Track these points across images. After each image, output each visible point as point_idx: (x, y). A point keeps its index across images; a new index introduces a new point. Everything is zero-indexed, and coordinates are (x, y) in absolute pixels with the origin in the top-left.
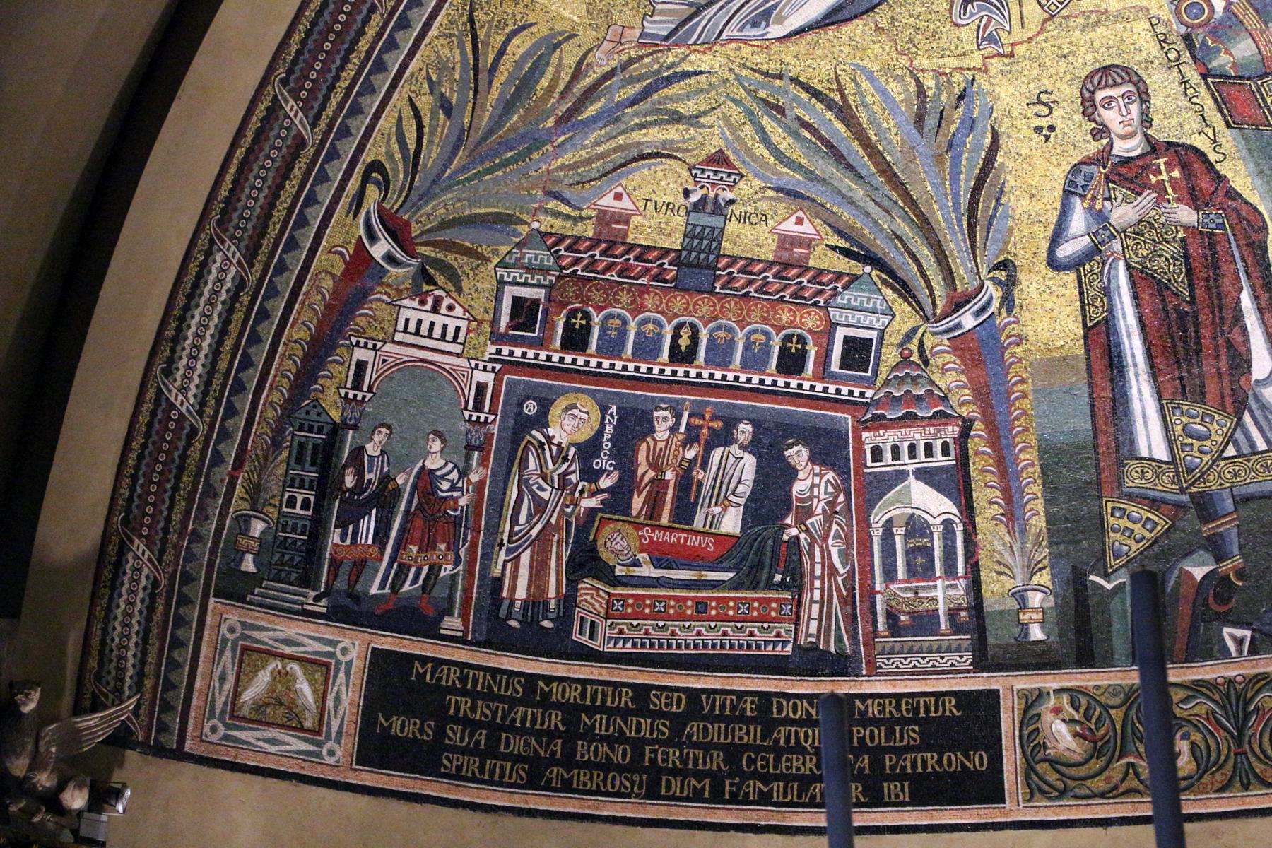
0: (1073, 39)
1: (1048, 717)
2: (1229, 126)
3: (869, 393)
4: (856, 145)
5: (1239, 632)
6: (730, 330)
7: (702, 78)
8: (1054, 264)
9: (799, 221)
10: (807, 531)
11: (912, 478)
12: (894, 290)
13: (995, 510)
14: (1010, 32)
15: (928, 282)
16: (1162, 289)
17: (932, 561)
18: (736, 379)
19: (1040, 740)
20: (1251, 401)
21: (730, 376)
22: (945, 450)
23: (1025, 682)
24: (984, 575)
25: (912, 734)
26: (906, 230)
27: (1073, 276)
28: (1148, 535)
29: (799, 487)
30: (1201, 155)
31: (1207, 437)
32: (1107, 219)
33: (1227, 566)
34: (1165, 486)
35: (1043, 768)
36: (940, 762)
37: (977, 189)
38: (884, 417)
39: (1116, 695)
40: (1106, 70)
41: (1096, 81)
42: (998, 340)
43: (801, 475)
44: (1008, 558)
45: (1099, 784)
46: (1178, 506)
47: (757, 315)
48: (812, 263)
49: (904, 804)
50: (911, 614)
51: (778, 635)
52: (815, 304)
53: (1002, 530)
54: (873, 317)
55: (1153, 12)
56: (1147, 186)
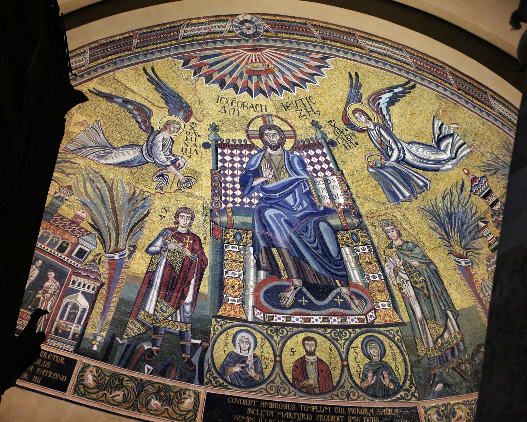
1: (88, 372)
2: (211, 236)
3: (79, 265)
4: (109, 199)
5: (150, 367)
6: (49, 234)
7: (76, 165)
8: (147, 251)
9: (83, 212)
10: (44, 297)
11: (80, 293)
12: (100, 240)
13: (100, 310)
15: (111, 242)
16: (173, 269)
17: (75, 318)
18: (44, 248)
19: (83, 378)
20: (181, 307)
21: (43, 246)
22: (93, 290)
23: (86, 360)
24: (88, 327)
25: (49, 364)
26: (111, 226)
27: (151, 256)
28: (138, 332)
29: (47, 284)
30: (200, 240)
31: (166, 312)
32: (167, 245)
33: (155, 348)
34: (148, 321)
35: (81, 386)
36: (52, 375)
37: (136, 224)
38: (80, 273)
39: (109, 373)
42: (122, 265)
43: (49, 281)
44: (97, 325)
45: (94, 396)
46: (149, 327)
47: (59, 232)
48: (81, 225)
49: (37, 384)
50: (63, 331)
51: (23, 323)
52: (76, 236)
53: (99, 317)
54: (90, 245)
56: (182, 241)
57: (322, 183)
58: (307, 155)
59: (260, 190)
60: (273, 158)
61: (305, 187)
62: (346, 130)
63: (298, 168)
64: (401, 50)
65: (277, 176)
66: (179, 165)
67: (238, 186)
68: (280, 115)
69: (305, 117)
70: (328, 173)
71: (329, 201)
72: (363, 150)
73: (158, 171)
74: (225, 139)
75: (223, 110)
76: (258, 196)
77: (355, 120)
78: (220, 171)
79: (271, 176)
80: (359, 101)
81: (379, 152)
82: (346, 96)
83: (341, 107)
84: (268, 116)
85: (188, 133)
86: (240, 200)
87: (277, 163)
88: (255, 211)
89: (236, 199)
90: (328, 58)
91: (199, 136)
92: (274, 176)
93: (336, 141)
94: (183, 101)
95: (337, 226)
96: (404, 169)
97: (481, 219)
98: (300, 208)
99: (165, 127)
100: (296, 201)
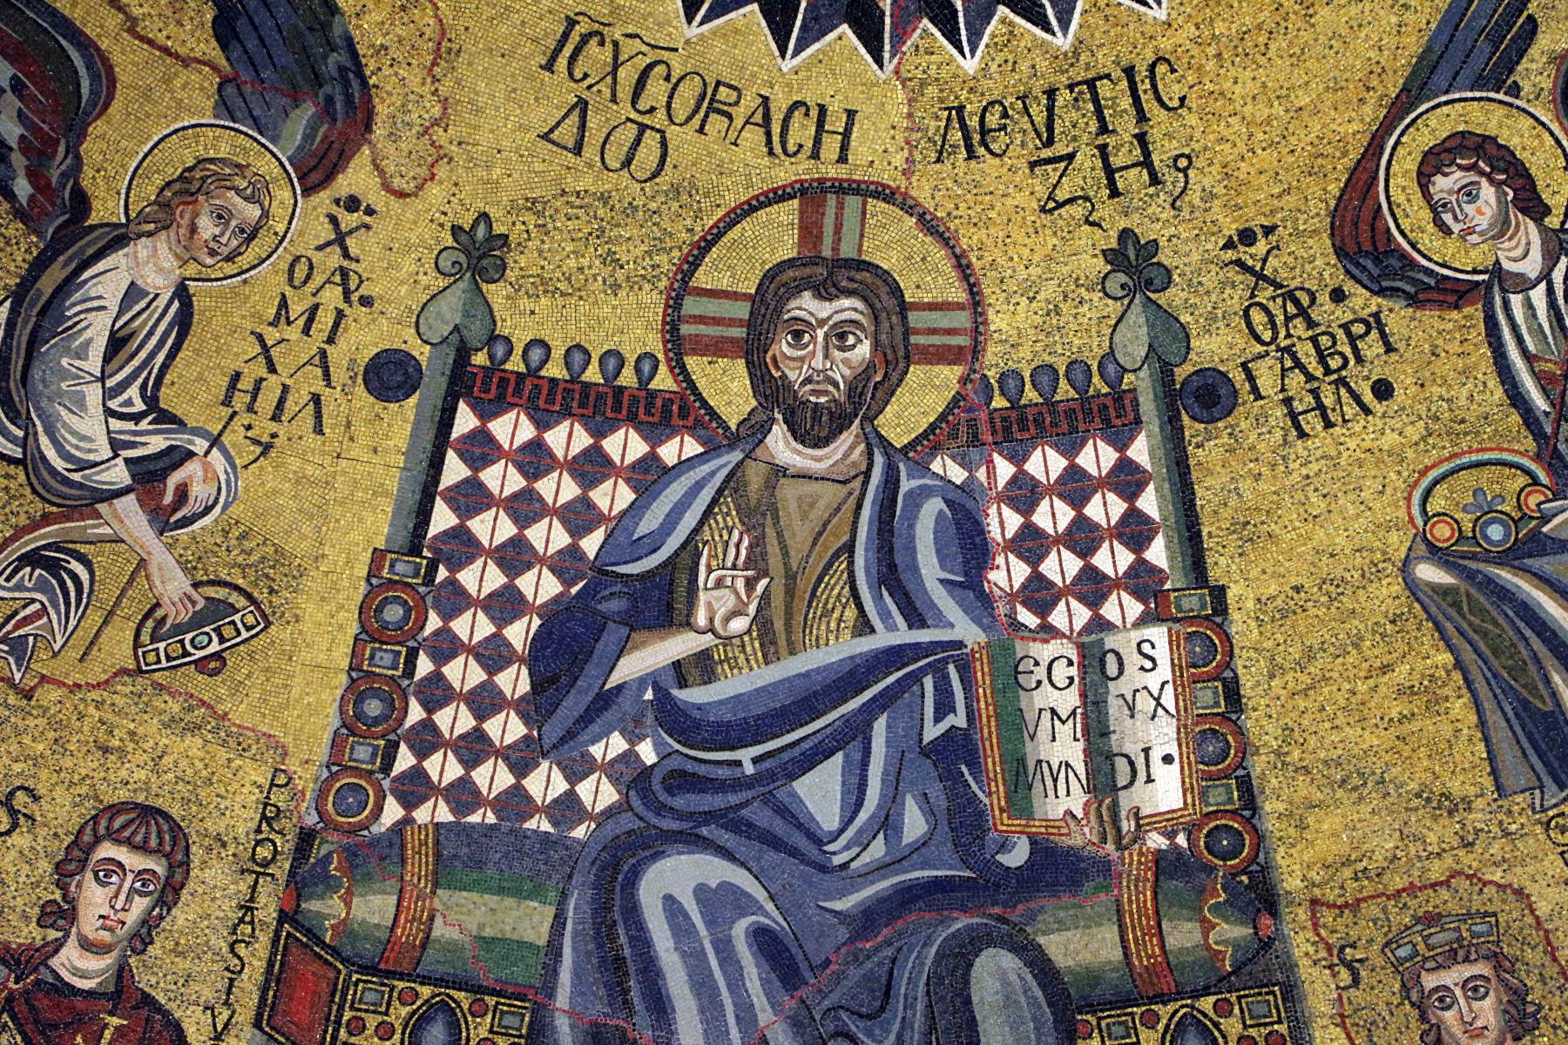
0: (141, 731)
2: (257, 1024)
14: (55, 655)
40: (148, 813)
41: (117, 824)
55: (292, 765)
57: (1061, 672)
58: (1013, 481)
59: (650, 719)
60: (789, 492)
61: (944, 707)
62: (1338, 296)
63: (930, 569)
65: (779, 625)
66: (182, 494)
67: (515, 681)
68: (922, 192)
69: (1078, 210)
70: (1122, 608)
71: (1076, 801)
72: (1414, 433)
73: (34, 526)
74: (520, 340)
75: (567, 133)
76: (629, 757)
77: (1426, 214)
78: (432, 567)
79: (739, 625)
81: (1530, 444)
82: (1414, 45)
83: (1354, 126)
84: (843, 188)
85: (300, 272)
86: (505, 779)
87: (799, 534)
88: (583, 864)
89: (481, 776)
91: (366, 301)
92: (762, 622)
93: (1238, 376)
94: (337, 31)
95: (1092, 977)
98: (878, 849)
99: (165, 206)
100: (859, 804)
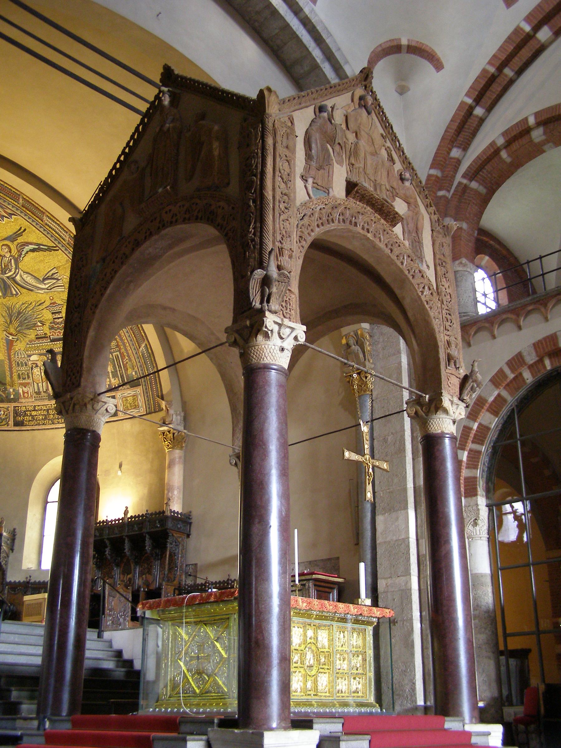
64: (67, 232)
80: (13, 242)
82: (6, 236)
90: (15, 215)
96: (9, 282)
97: (40, 322)
